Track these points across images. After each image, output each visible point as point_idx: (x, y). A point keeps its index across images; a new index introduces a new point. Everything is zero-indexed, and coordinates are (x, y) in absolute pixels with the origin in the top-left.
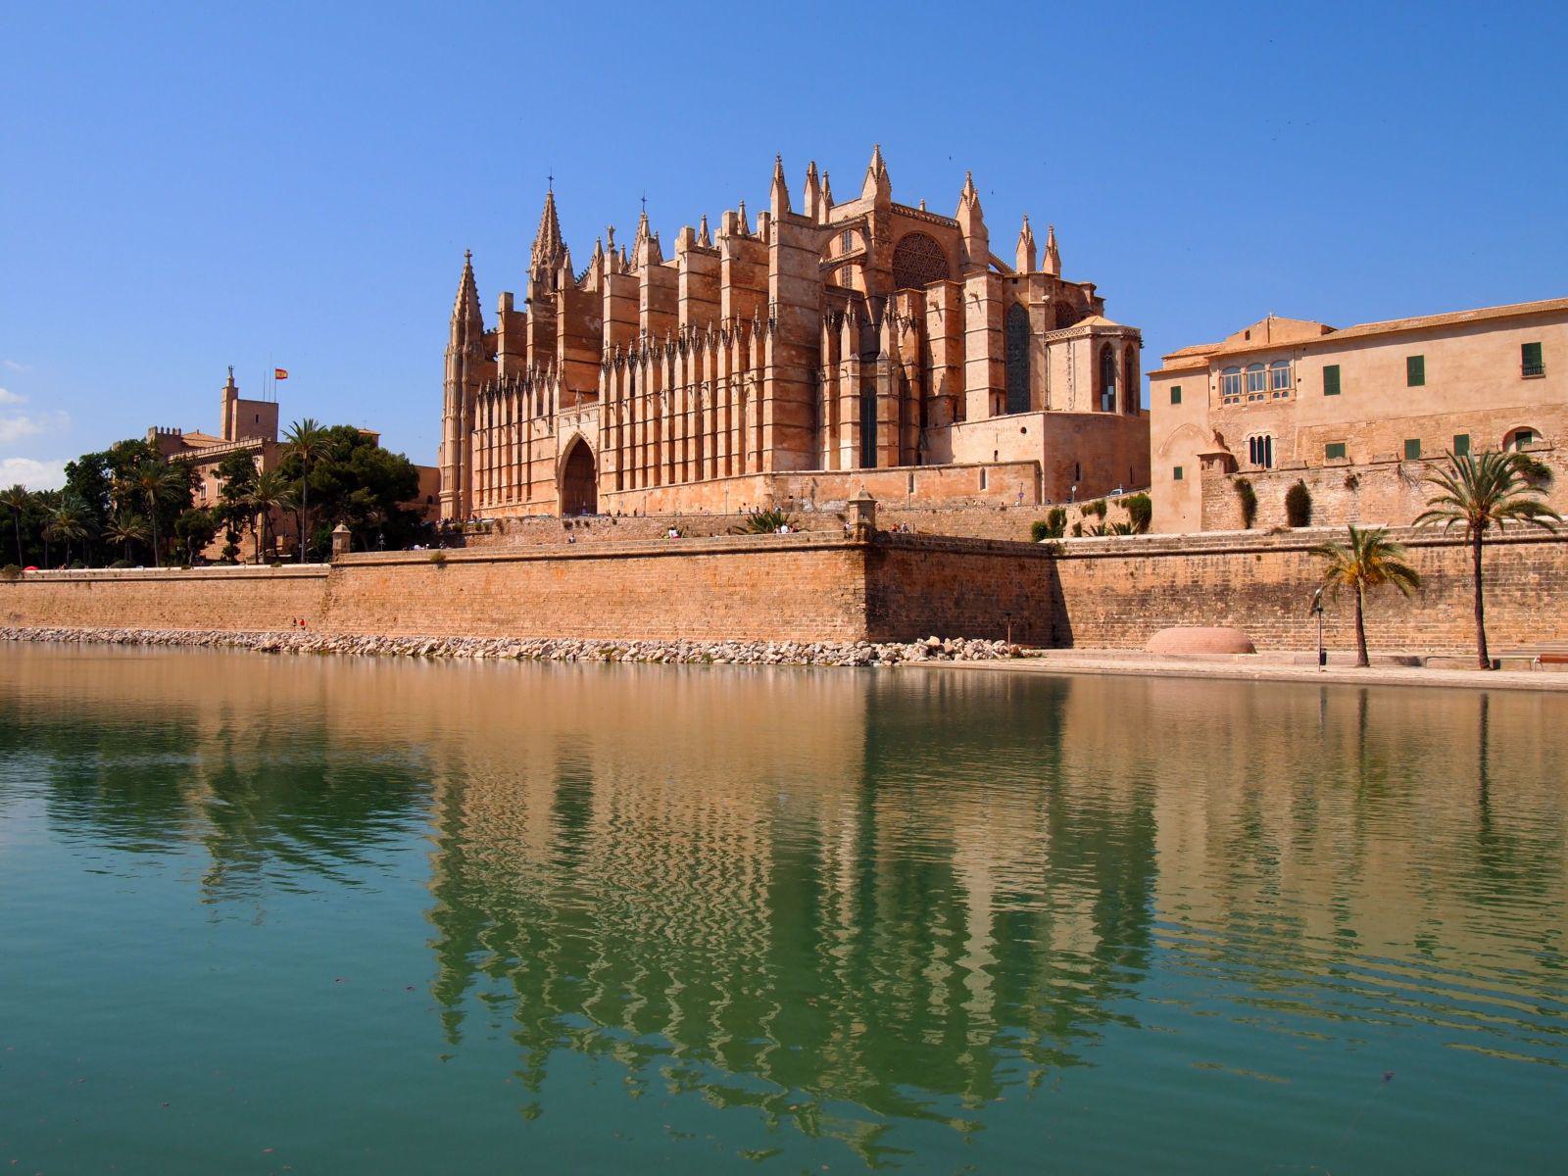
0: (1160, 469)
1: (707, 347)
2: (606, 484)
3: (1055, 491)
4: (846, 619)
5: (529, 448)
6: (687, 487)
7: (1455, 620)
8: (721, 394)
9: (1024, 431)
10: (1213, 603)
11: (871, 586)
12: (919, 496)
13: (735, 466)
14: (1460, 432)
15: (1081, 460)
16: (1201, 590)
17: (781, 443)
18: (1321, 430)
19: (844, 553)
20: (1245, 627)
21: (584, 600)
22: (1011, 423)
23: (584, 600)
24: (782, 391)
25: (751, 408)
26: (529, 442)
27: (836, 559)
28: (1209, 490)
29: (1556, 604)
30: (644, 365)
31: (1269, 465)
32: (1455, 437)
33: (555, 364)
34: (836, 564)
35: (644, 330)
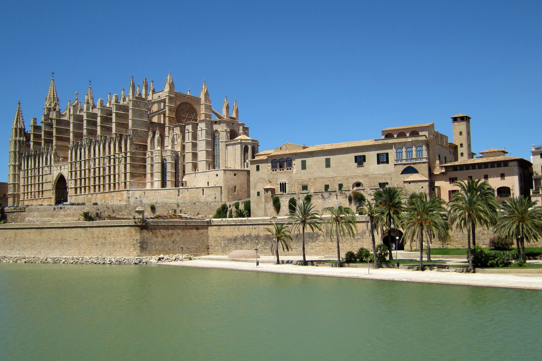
0: (253, 192)
1: (107, 143)
2: (71, 192)
3: (227, 196)
4: (134, 249)
5: (42, 177)
6: (100, 194)
7: (320, 246)
8: (112, 161)
9: (217, 175)
10: (255, 241)
11: (142, 238)
12: (181, 198)
13: (117, 187)
14: (340, 183)
15: (236, 186)
16: (251, 236)
17: (133, 179)
18: (300, 181)
19: (133, 228)
20: (264, 248)
21: (49, 242)
22: (213, 173)
23: (49, 242)
24: (133, 160)
25: (122, 166)
26: (42, 176)
27: (131, 229)
28: (267, 200)
29: (347, 241)
30: (85, 149)
31: (285, 192)
32: (339, 184)
33: (52, 147)
34: (131, 231)
35: (85, 136)
